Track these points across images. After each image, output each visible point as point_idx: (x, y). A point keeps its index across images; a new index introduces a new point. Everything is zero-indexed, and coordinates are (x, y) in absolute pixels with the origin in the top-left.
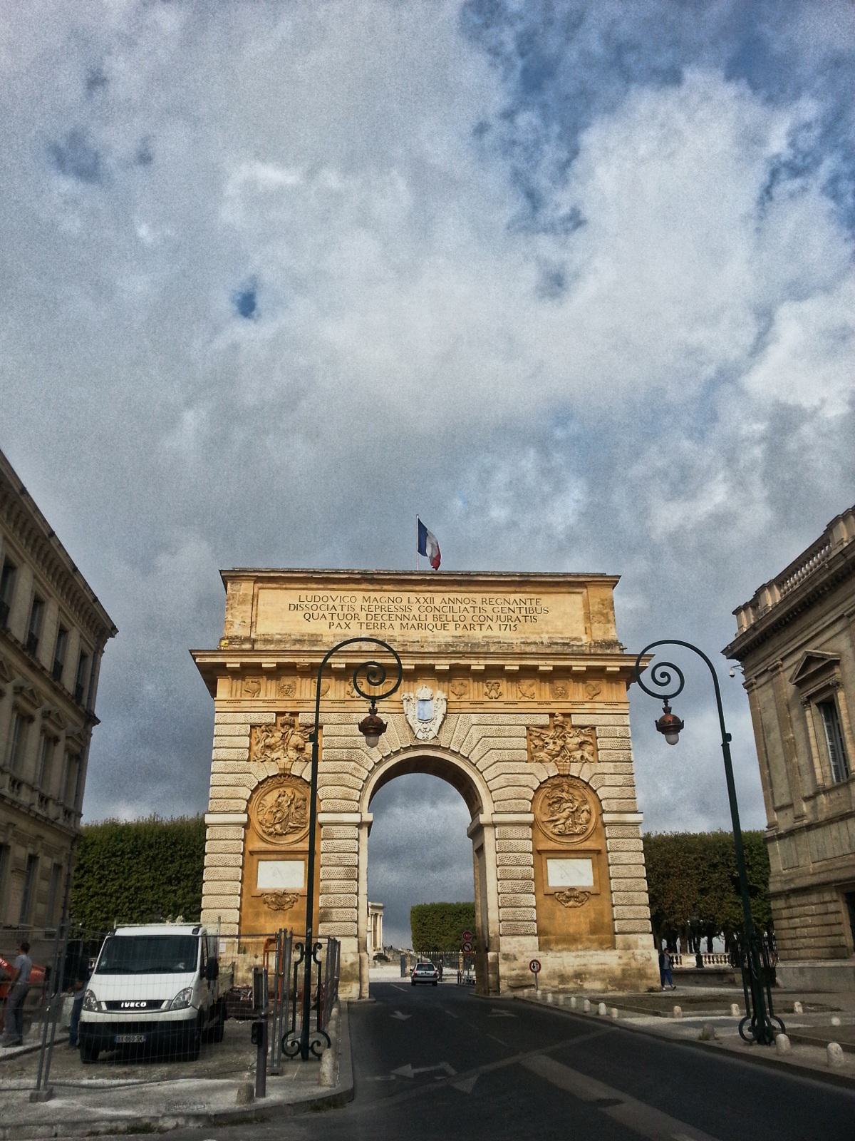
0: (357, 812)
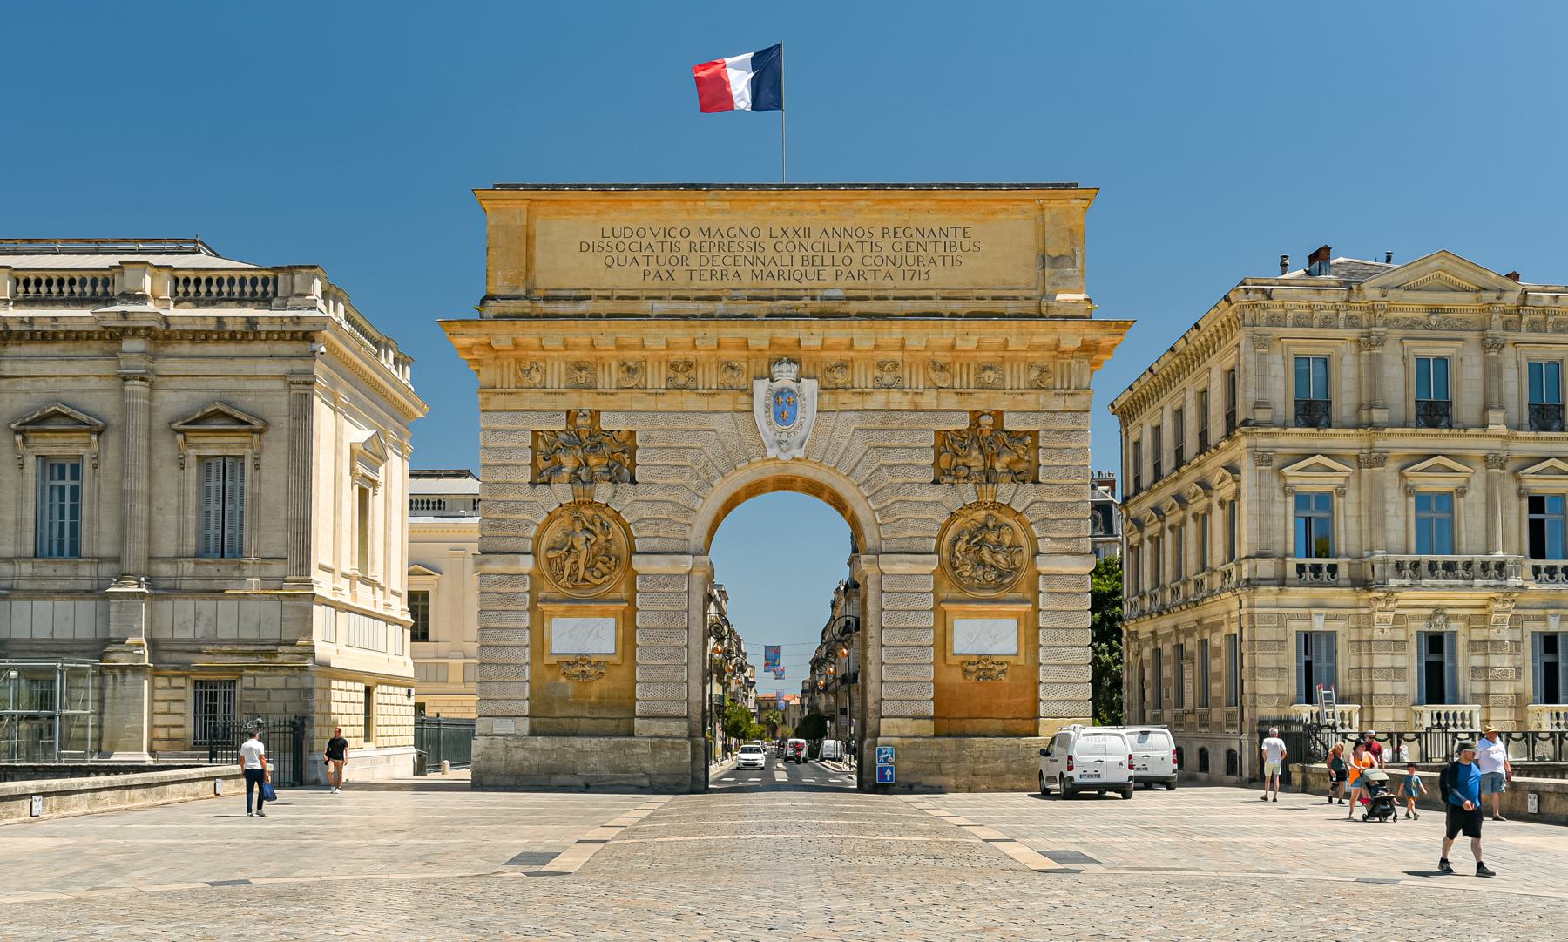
0: (685, 553)
